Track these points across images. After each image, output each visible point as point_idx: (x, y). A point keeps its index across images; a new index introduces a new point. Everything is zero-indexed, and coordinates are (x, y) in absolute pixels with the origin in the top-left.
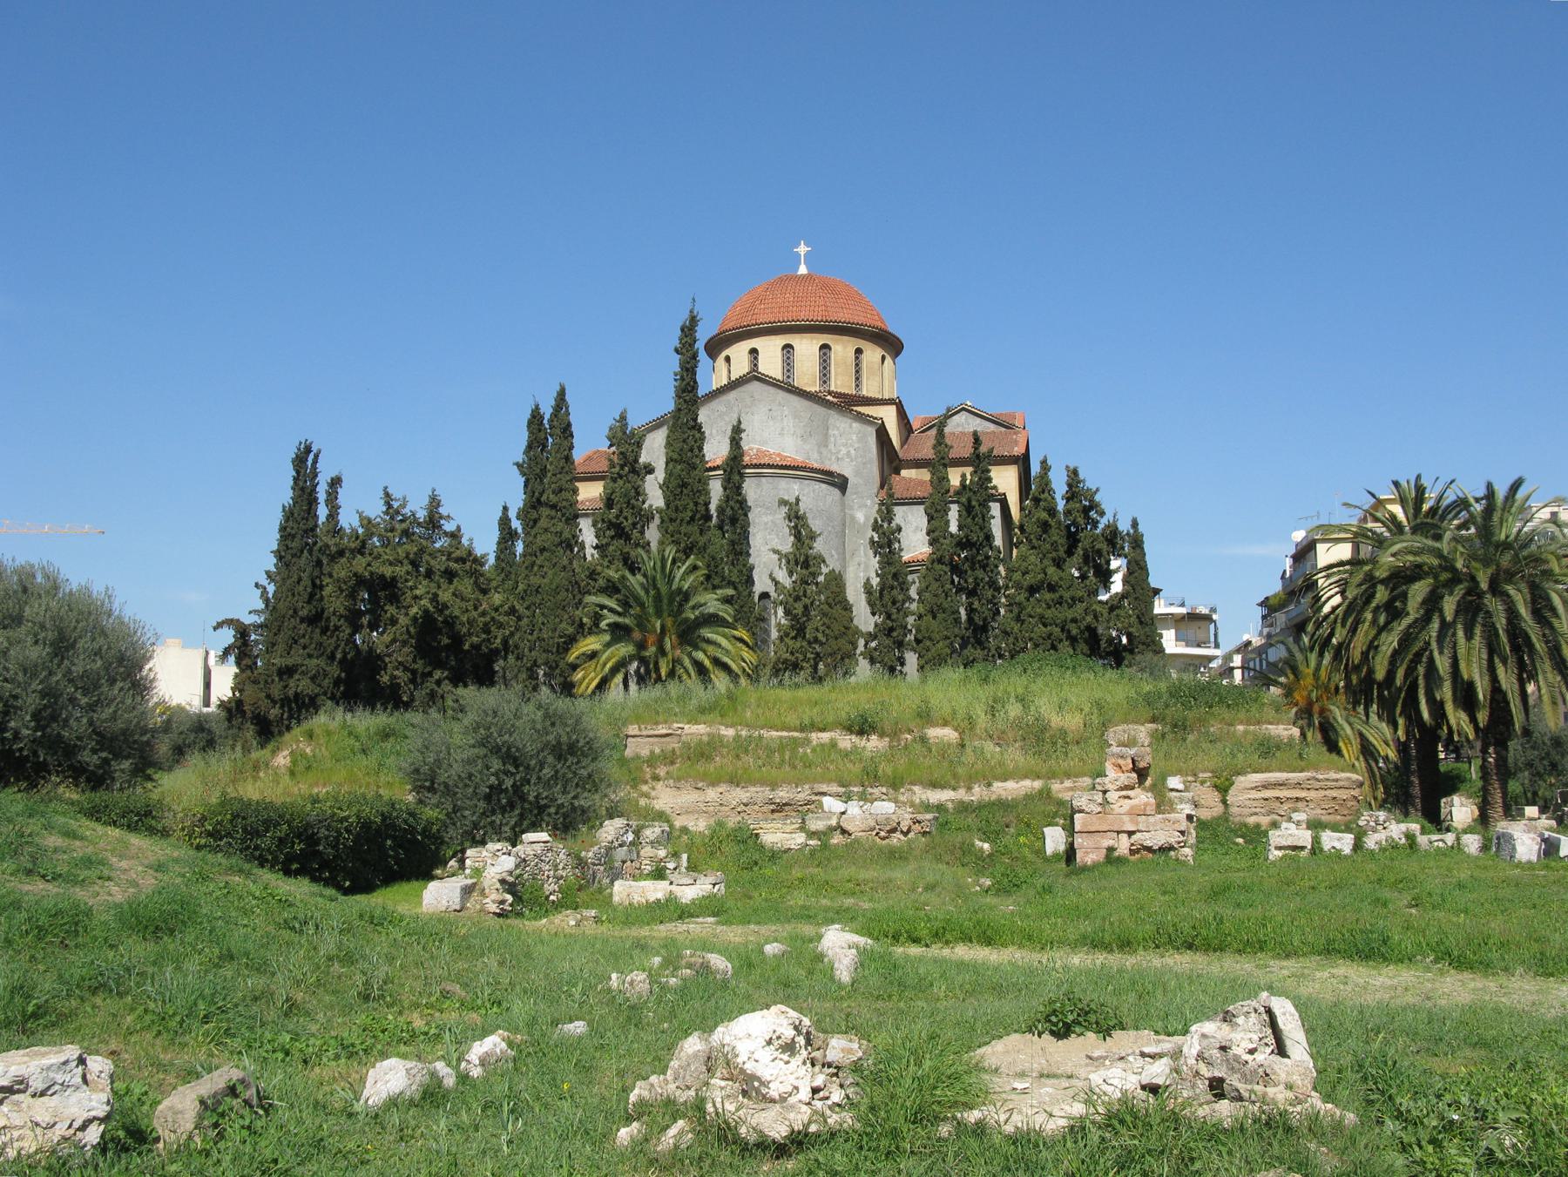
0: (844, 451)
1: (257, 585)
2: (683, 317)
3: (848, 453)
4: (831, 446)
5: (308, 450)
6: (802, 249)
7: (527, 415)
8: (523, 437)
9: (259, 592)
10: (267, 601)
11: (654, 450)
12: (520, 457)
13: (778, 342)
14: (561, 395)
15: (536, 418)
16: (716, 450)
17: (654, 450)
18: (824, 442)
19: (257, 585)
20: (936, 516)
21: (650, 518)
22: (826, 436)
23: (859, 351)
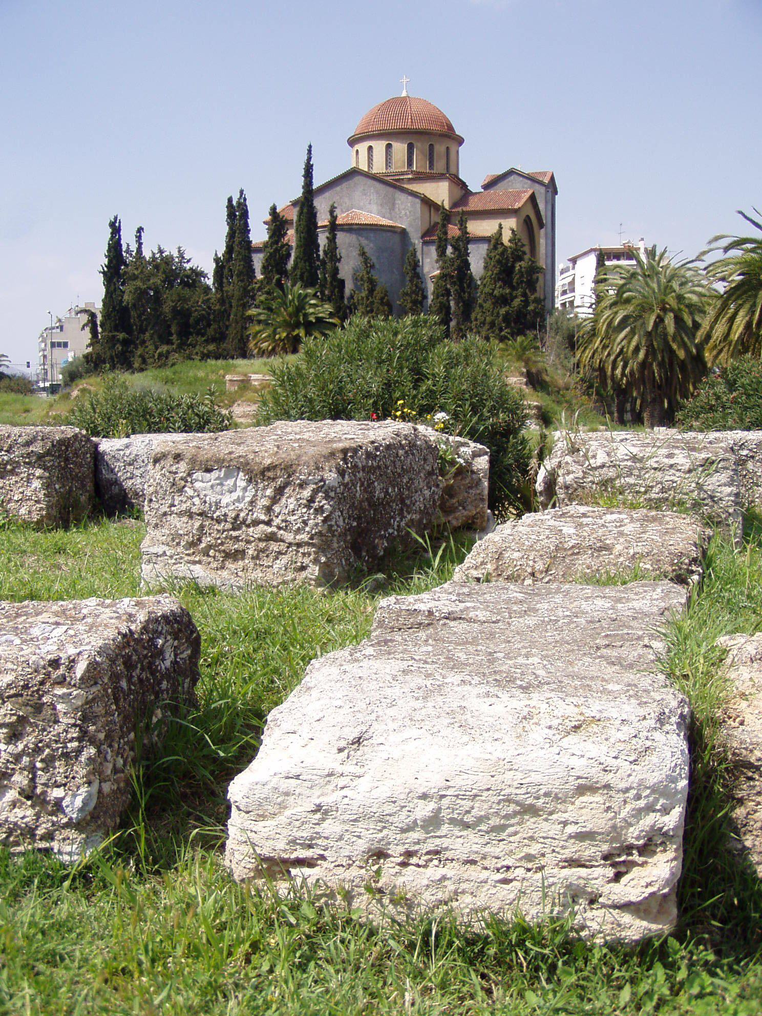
0: (403, 212)
3: (406, 214)
4: (397, 210)
5: (116, 218)
14: (242, 192)
15: (230, 200)
16: (323, 220)
18: (393, 207)
22: (394, 204)
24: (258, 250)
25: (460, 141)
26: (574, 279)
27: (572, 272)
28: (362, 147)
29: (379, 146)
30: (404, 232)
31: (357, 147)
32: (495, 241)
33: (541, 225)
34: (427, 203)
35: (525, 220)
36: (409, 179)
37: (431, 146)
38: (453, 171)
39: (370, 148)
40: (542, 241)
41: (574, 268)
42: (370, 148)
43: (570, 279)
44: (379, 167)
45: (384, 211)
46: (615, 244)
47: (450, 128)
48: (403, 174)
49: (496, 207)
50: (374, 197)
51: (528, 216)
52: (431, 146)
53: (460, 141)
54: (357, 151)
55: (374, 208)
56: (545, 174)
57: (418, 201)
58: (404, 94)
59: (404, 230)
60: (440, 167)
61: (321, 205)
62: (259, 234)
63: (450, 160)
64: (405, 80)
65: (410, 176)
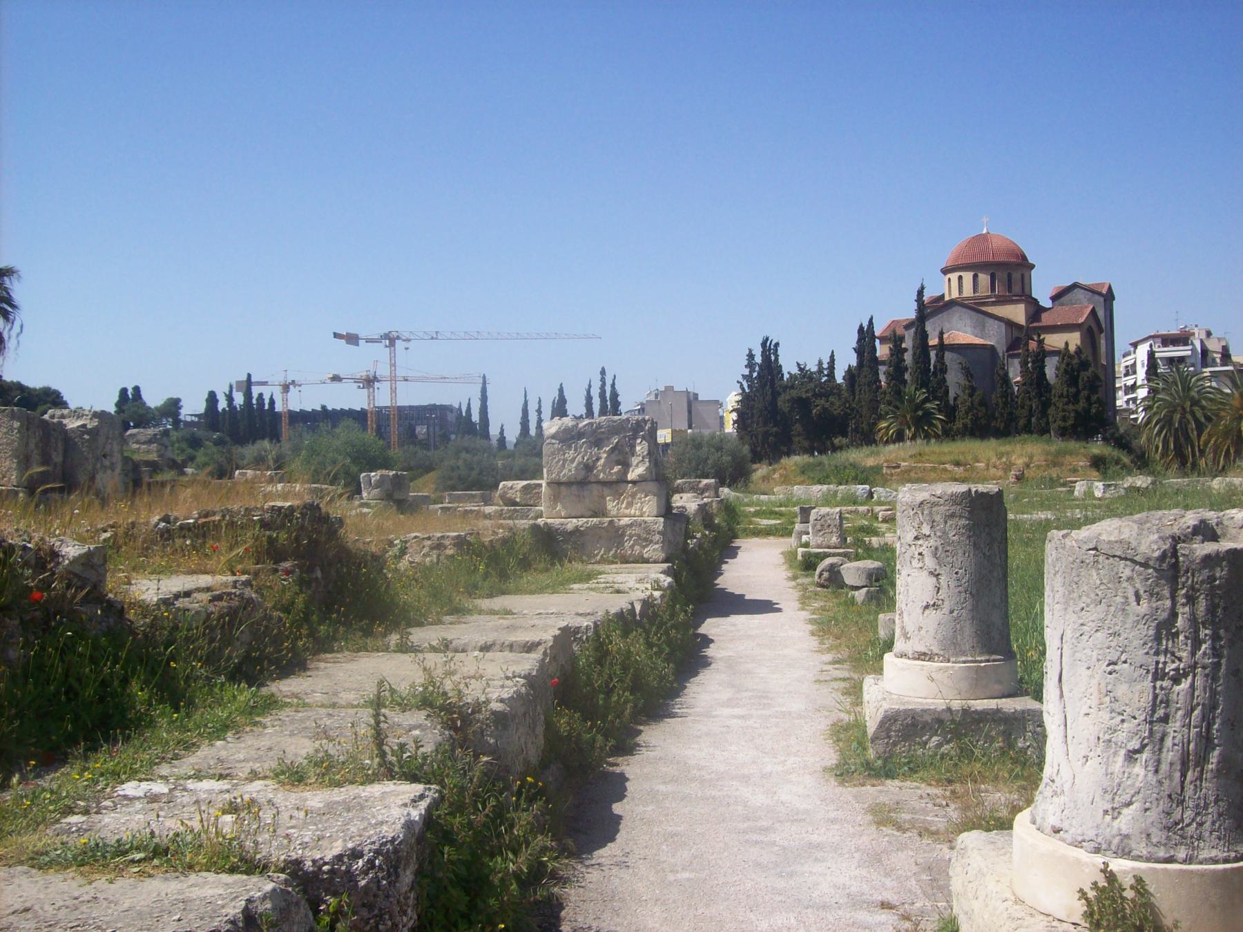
1: (738, 382)
2: (918, 287)
4: (987, 331)
5: (767, 339)
6: (985, 220)
7: (858, 328)
8: (855, 337)
9: (739, 385)
10: (743, 389)
11: (908, 344)
12: (855, 345)
15: (861, 329)
16: (933, 341)
17: (908, 344)
19: (738, 382)
20: (1024, 364)
21: (906, 369)
22: (984, 326)
24: (883, 363)
25: (1032, 267)
26: (1135, 362)
27: (1132, 356)
28: (954, 277)
29: (968, 277)
30: (992, 349)
31: (949, 276)
32: (1063, 353)
33: (1101, 331)
34: (1010, 324)
35: (1088, 330)
36: (993, 302)
37: (1009, 276)
38: (1027, 291)
39: (960, 278)
40: (1103, 342)
41: (1135, 352)
43: (1132, 361)
44: (968, 291)
45: (976, 332)
46: (1174, 331)
47: (1024, 258)
48: (988, 297)
49: (1063, 322)
50: (968, 322)
51: (1090, 327)
52: (1009, 276)
53: (1032, 267)
54: (949, 279)
55: (969, 329)
56: (1103, 285)
57: (1003, 326)
58: (985, 231)
59: (993, 346)
60: (1017, 289)
61: (931, 328)
62: (882, 351)
63: (1025, 284)
64: (985, 220)
65: (993, 300)
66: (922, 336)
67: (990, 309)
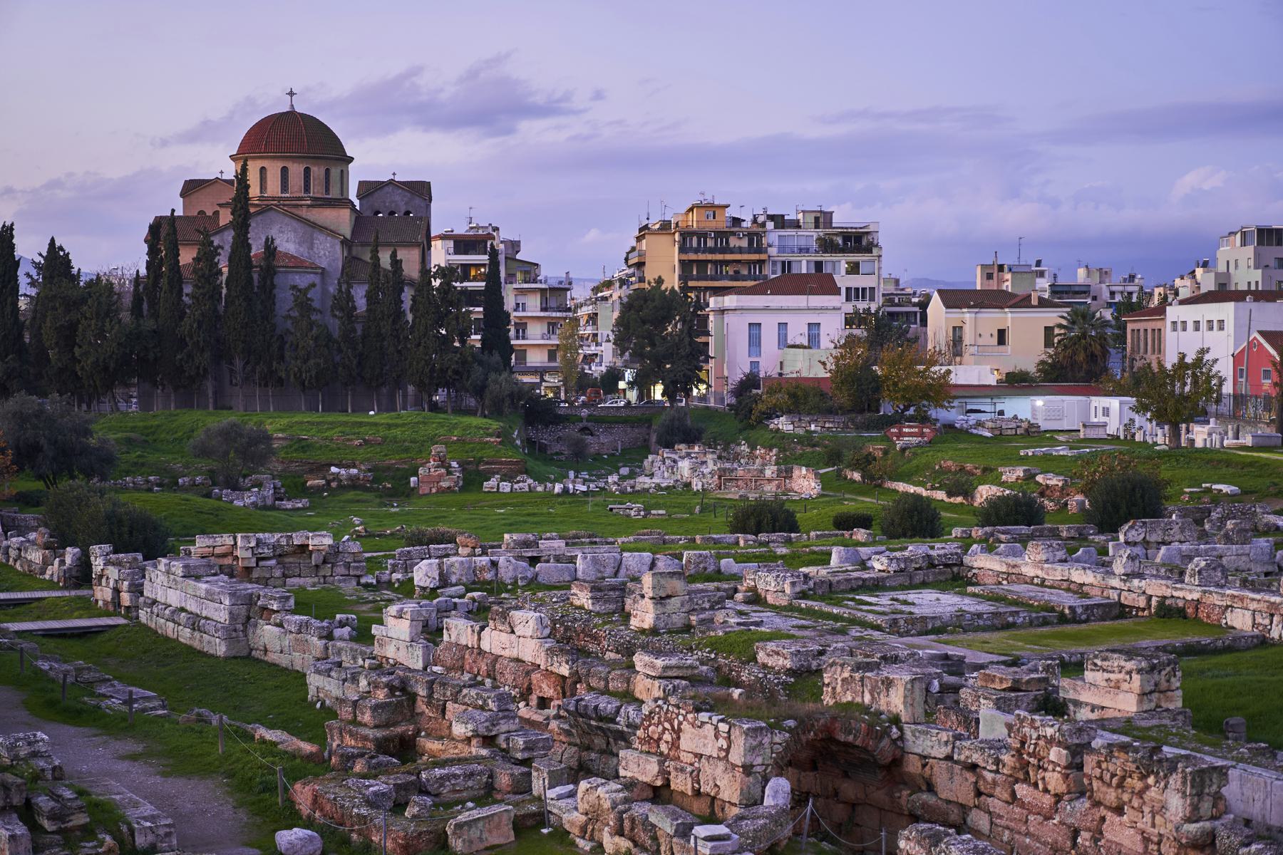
4: (315, 250)
13: (280, 164)
18: (311, 247)
23: (327, 171)
29: (274, 169)
36: (309, 206)
42: (263, 169)
50: (291, 235)
65: (309, 202)
66: (242, 244)
67: (304, 213)
